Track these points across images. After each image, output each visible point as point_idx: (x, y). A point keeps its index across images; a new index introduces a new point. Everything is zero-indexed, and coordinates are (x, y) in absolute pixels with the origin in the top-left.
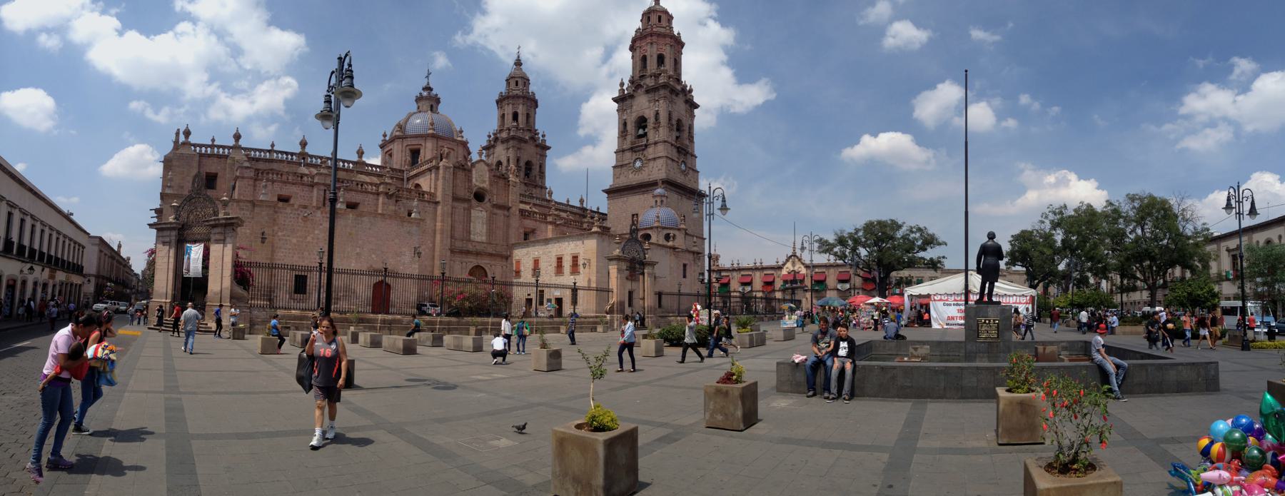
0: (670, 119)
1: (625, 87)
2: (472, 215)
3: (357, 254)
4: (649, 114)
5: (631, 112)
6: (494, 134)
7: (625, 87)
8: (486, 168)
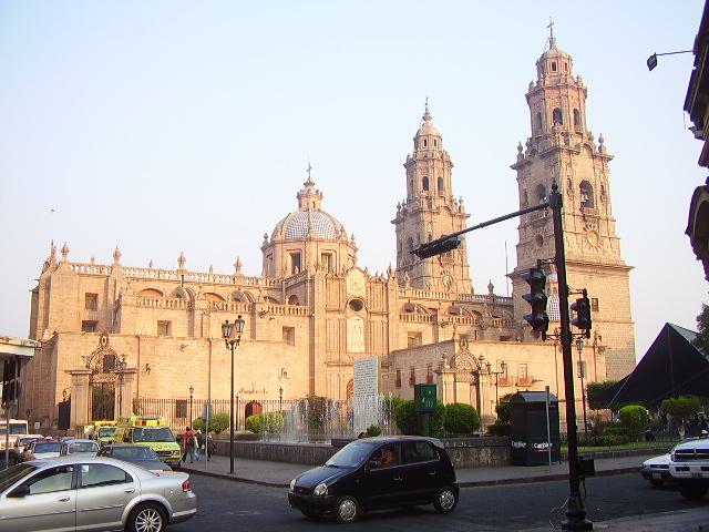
1: (523, 152)
7: (523, 152)
8: (362, 274)
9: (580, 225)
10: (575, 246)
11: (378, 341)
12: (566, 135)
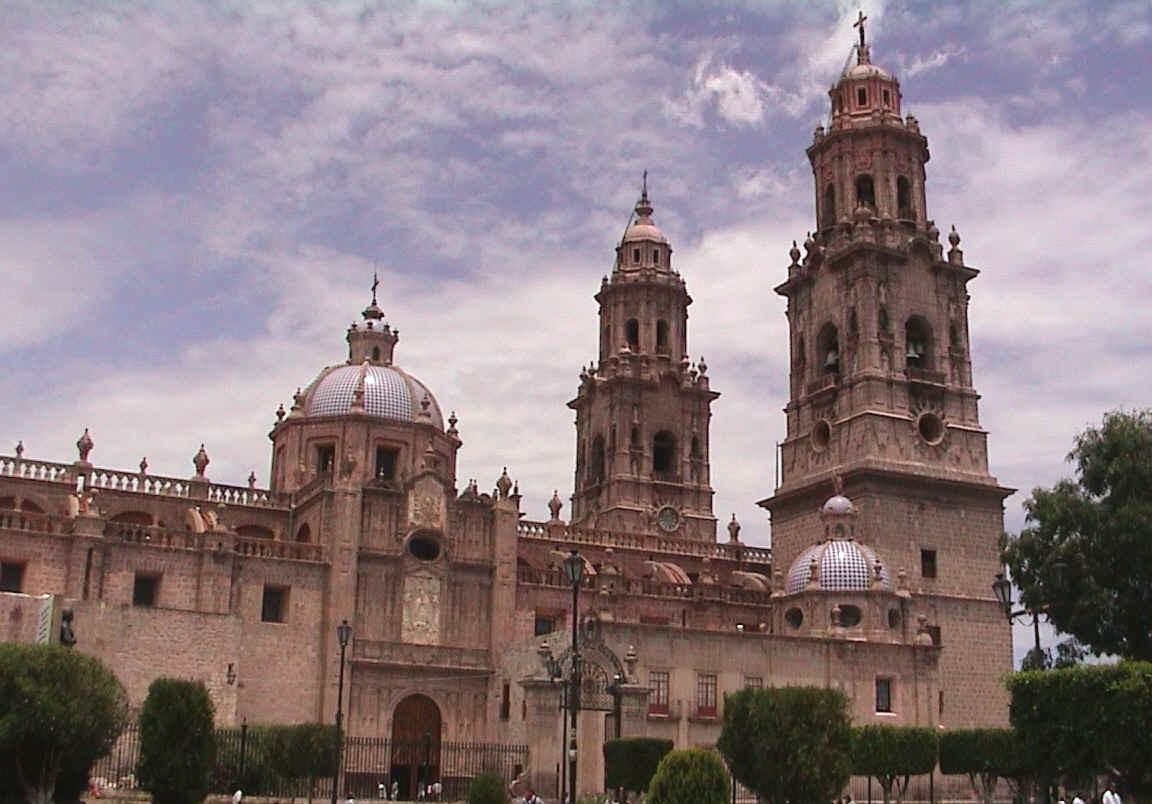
4: (839, 317)
5: (811, 317)
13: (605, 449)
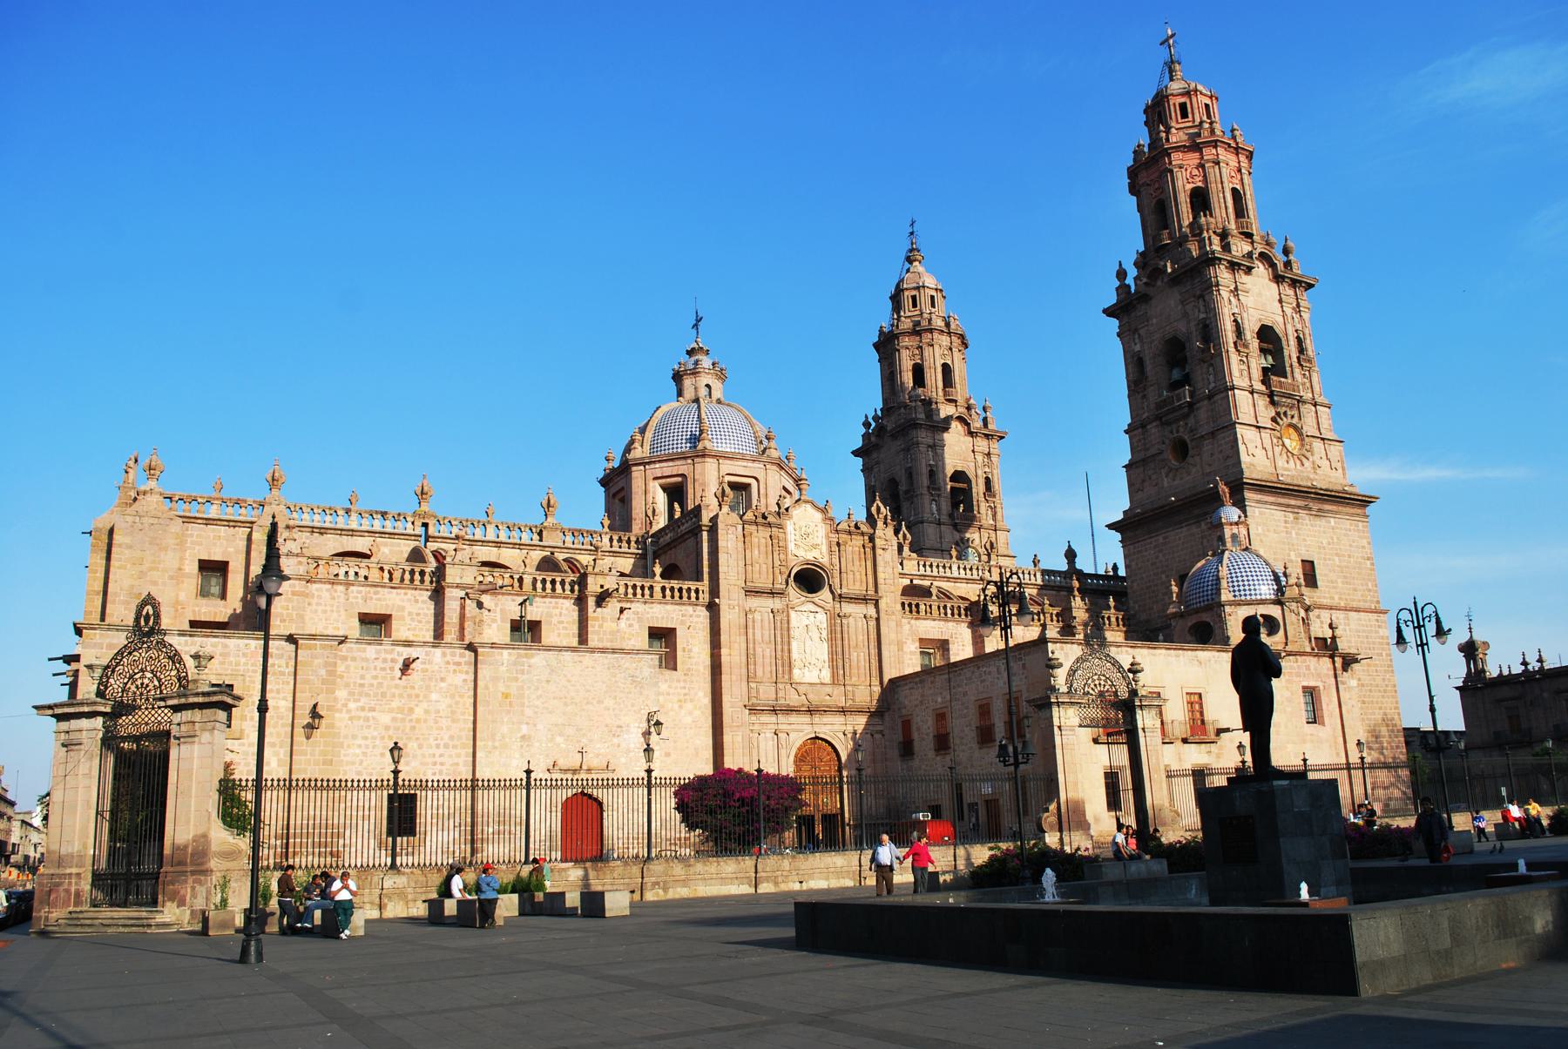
0: (1239, 331)
1: (1130, 281)
2: (793, 623)
3: (523, 737)
6: (875, 418)
7: (1130, 281)
8: (819, 516)
9: (1266, 413)
10: (1260, 453)
11: (859, 656)
12: (1224, 235)
13: (901, 492)
